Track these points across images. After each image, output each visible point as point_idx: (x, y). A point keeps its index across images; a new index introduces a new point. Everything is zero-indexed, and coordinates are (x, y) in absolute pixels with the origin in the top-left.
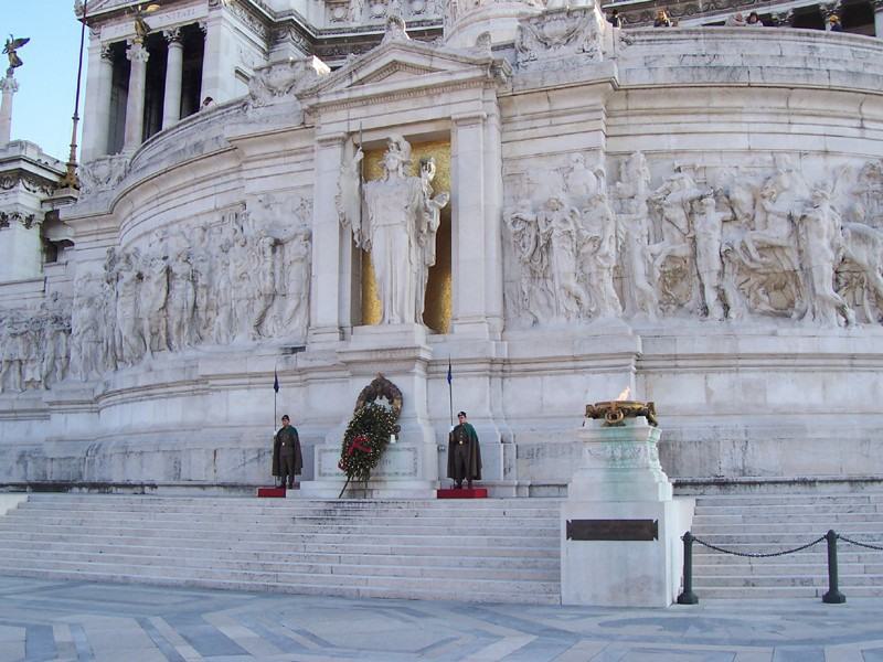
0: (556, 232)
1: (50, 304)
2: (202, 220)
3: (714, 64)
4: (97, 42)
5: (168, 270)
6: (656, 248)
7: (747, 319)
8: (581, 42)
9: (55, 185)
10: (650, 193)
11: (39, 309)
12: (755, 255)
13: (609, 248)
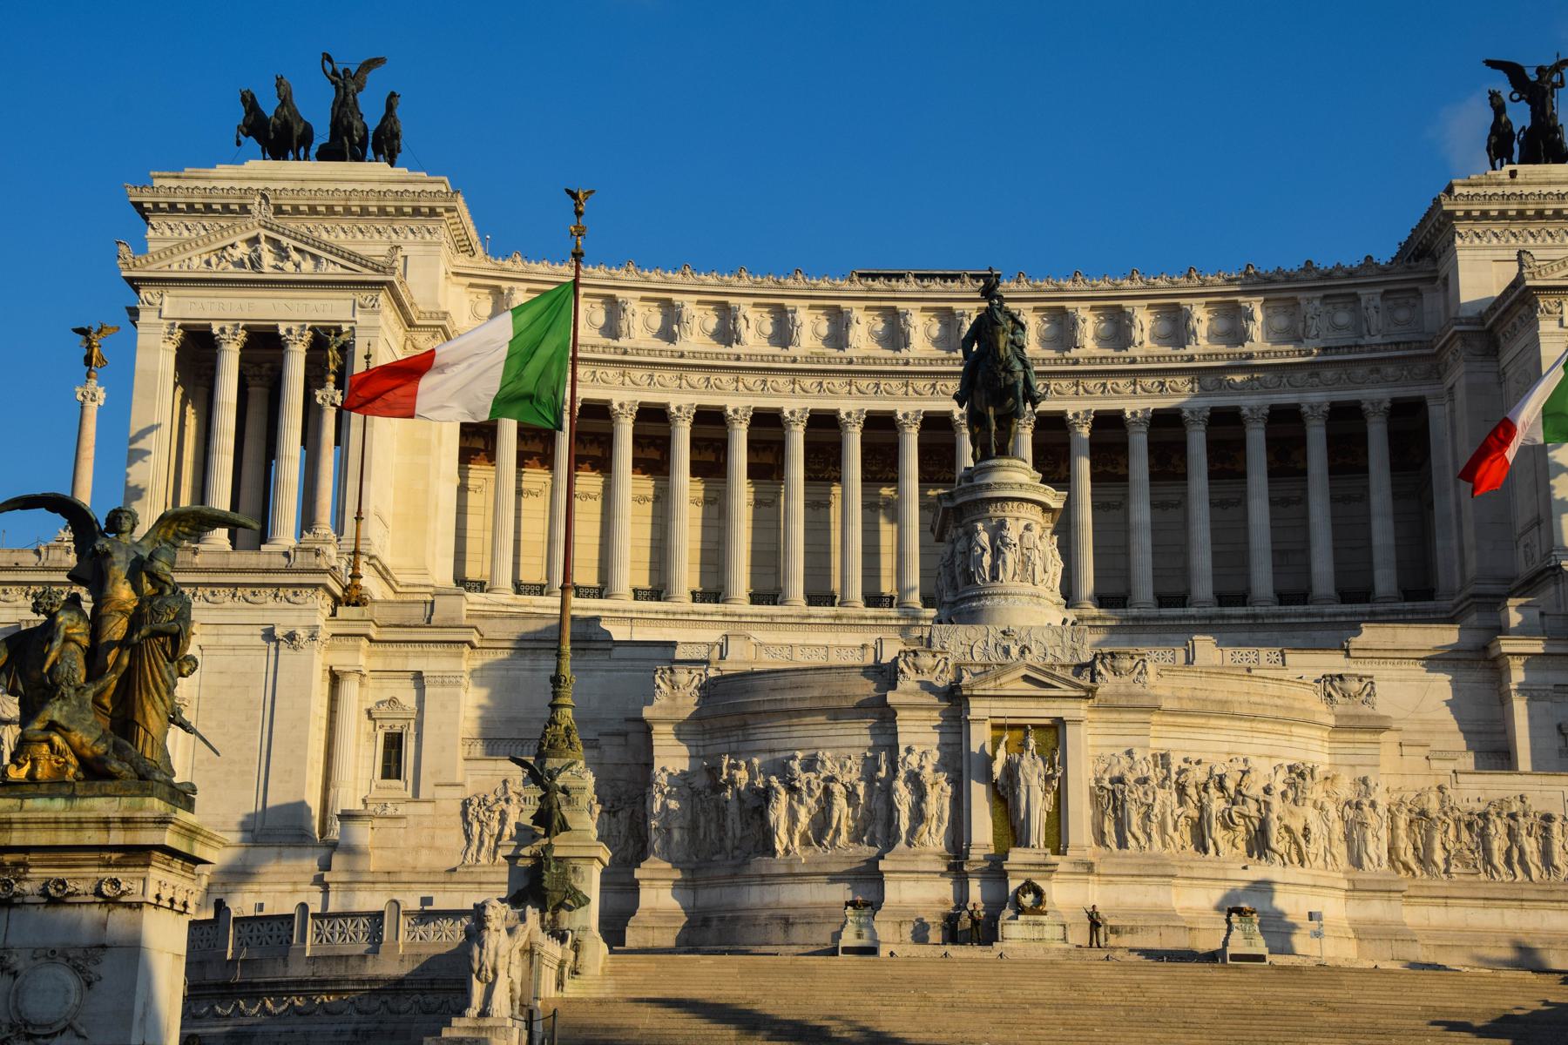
5: (826, 789)
9: (337, 601)
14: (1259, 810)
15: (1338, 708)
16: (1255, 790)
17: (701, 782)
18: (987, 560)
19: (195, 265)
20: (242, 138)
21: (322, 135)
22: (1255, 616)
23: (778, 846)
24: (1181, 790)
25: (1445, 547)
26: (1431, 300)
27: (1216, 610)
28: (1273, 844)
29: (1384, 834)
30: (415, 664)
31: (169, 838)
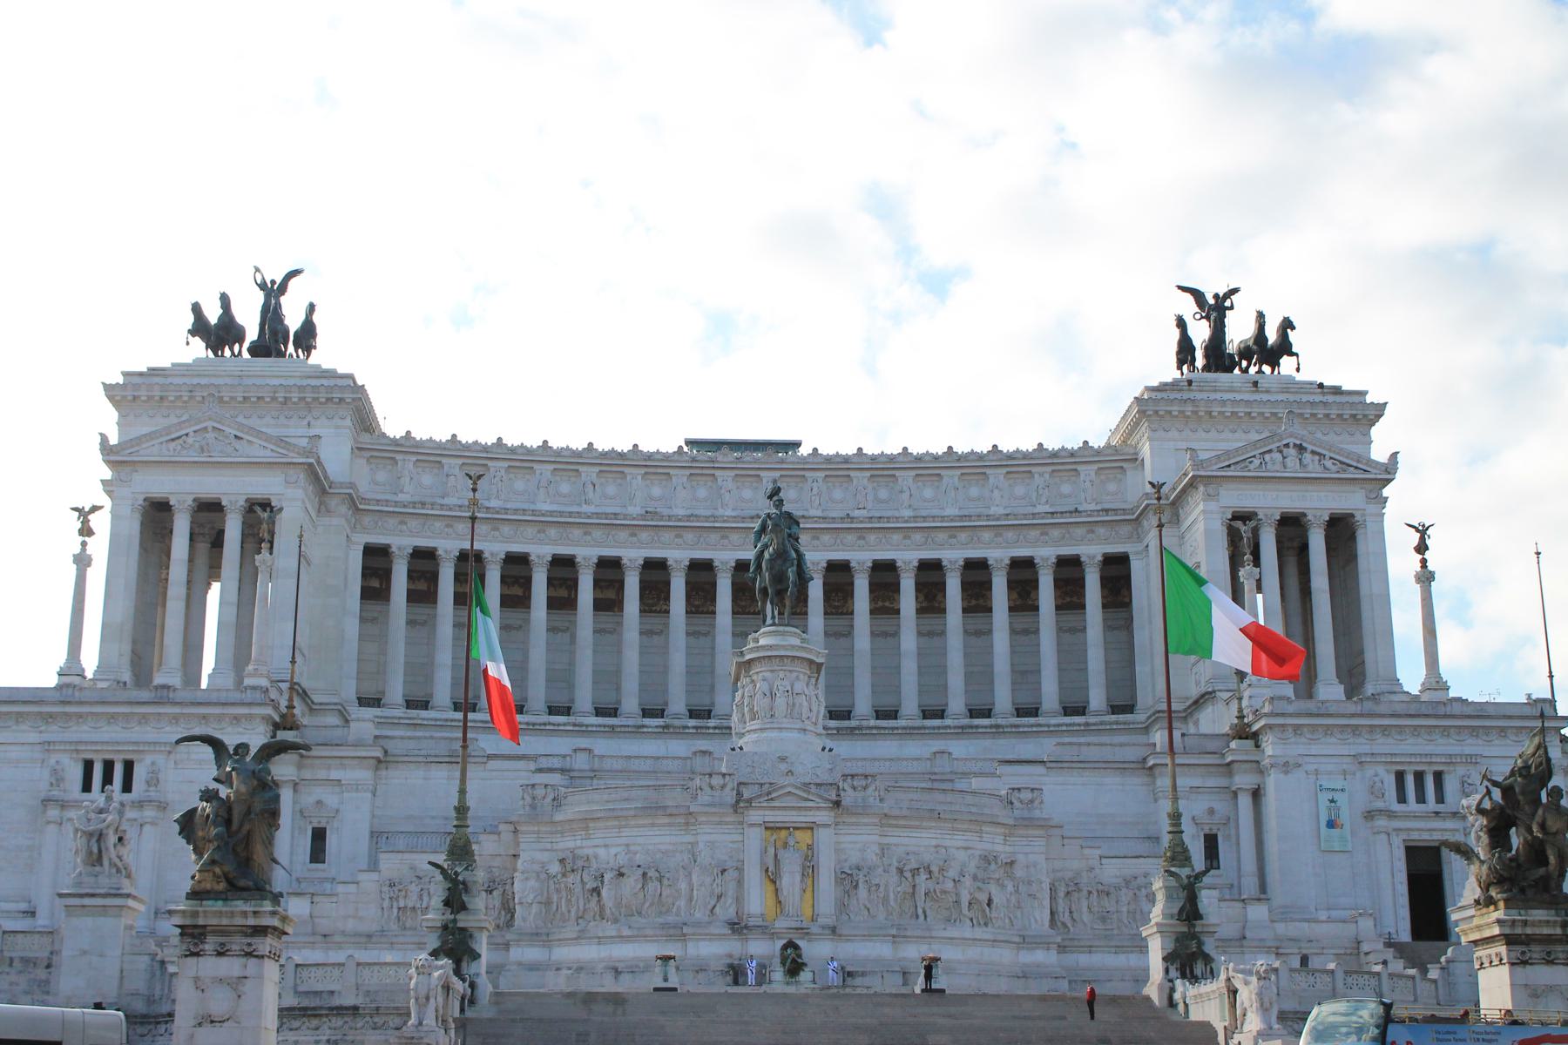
2: (663, 847)
5: (644, 874)
16: (952, 873)
17: (555, 868)
18: (767, 700)
19: (152, 451)
21: (252, 334)
22: (997, 726)
26: (1131, 475)
27: (967, 721)
28: (965, 911)
29: (1047, 903)
30: (334, 775)
31: (276, 922)
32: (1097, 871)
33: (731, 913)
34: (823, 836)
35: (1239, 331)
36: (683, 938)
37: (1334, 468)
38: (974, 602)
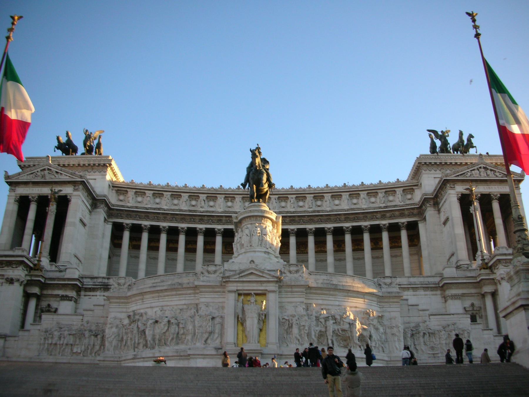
0: (294, 323)
1: (85, 325)
2: (181, 307)
3: (331, 283)
4: (13, 194)
6: (317, 329)
7: (338, 348)
8: (300, 274)
9: (31, 269)
10: (316, 315)
11: (79, 326)
12: (341, 332)
13: (307, 328)
14: (350, 327)
15: (383, 290)
17: (126, 322)
20: (56, 149)
21: (81, 149)
23: (149, 345)
24: (317, 319)
25: (426, 266)
29: (402, 339)
32: (428, 323)
33: (217, 343)
34: (272, 297)
35: (452, 140)
36: (188, 357)
37: (501, 176)
38: (356, 247)
